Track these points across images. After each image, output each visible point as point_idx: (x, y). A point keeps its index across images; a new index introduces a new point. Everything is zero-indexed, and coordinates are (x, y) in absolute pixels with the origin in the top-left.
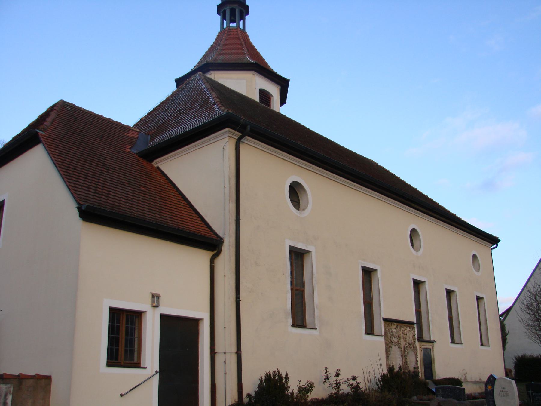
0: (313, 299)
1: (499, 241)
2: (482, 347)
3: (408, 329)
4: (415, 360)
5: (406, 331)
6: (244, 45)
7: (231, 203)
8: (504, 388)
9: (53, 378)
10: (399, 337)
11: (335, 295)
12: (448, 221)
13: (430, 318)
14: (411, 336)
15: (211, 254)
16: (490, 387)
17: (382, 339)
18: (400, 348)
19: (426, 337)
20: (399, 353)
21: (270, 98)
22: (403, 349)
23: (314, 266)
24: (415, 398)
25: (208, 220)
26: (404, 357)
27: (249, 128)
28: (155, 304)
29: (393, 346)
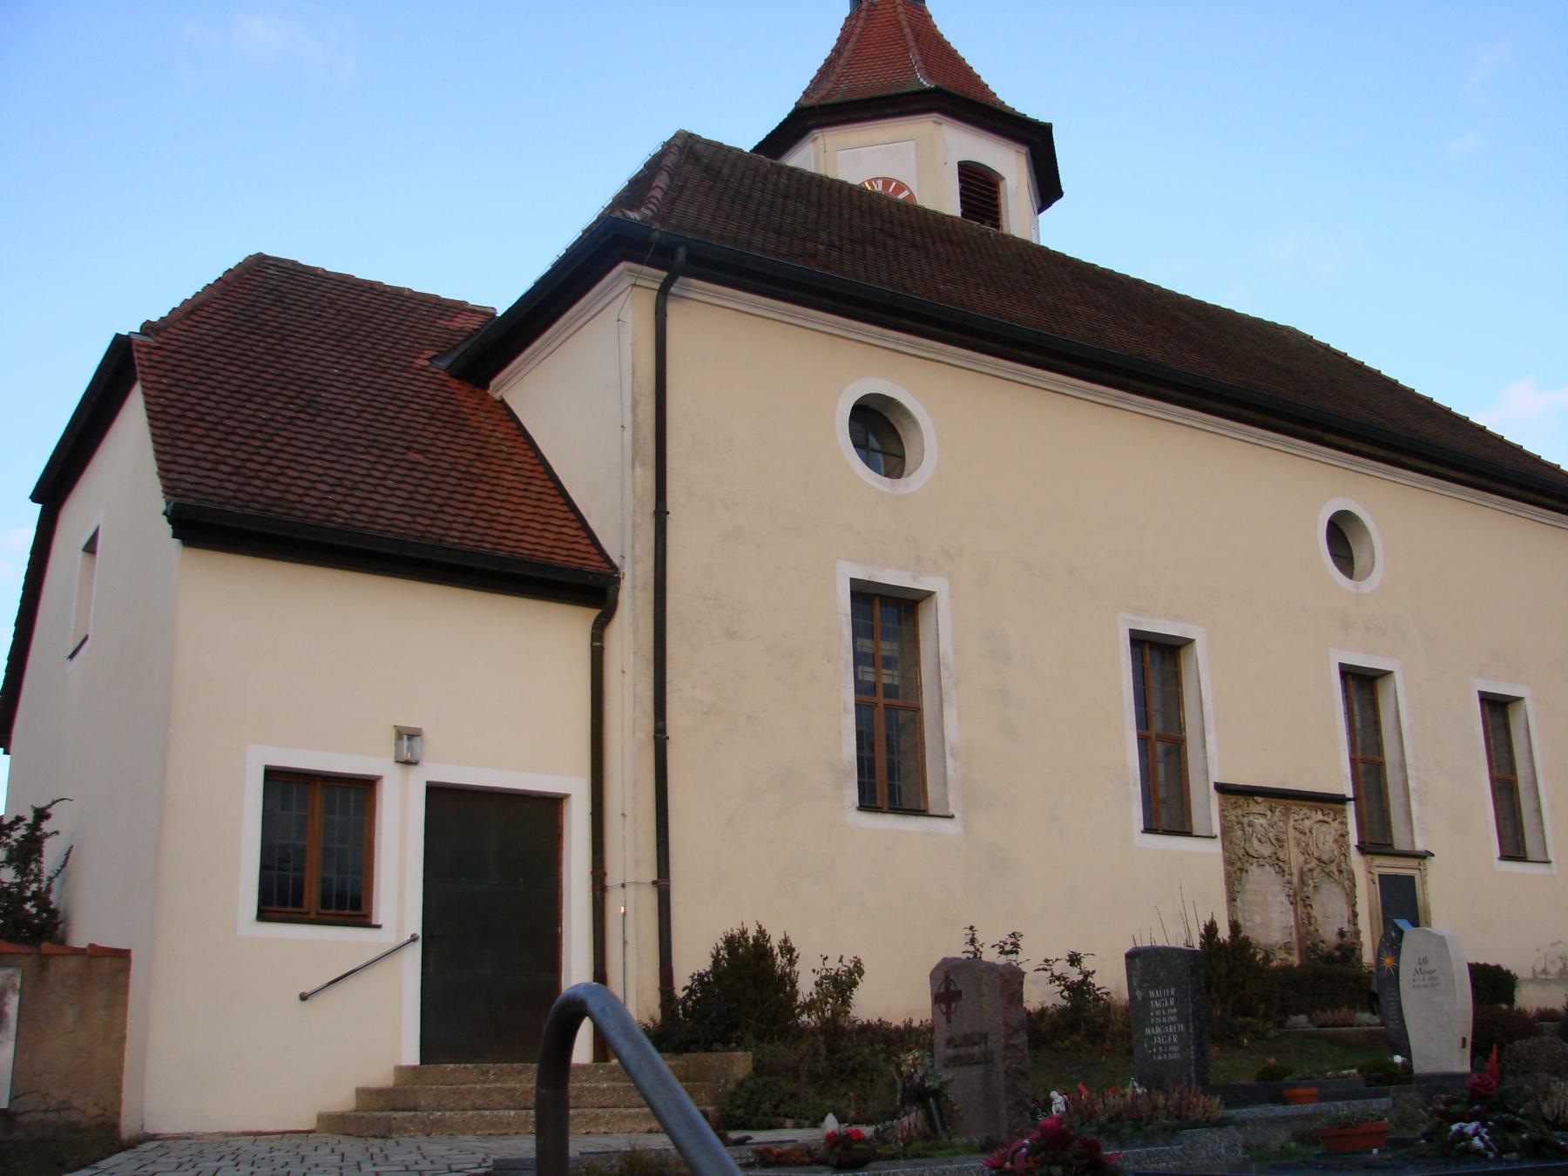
0: (942, 732)
3: (1320, 816)
4: (1345, 911)
5: (1307, 823)
6: (912, 44)
7: (639, 470)
8: (1425, 961)
9: (134, 955)
11: (1030, 720)
12: (1482, 481)
13: (1412, 784)
14: (1330, 838)
15: (591, 614)
16: (1388, 961)
17: (1216, 847)
19: (1400, 843)
22: (1295, 879)
23: (945, 635)
24: (1302, 1019)
25: (593, 523)
26: (1300, 899)
27: (681, 254)
28: (407, 756)
29: (1254, 870)
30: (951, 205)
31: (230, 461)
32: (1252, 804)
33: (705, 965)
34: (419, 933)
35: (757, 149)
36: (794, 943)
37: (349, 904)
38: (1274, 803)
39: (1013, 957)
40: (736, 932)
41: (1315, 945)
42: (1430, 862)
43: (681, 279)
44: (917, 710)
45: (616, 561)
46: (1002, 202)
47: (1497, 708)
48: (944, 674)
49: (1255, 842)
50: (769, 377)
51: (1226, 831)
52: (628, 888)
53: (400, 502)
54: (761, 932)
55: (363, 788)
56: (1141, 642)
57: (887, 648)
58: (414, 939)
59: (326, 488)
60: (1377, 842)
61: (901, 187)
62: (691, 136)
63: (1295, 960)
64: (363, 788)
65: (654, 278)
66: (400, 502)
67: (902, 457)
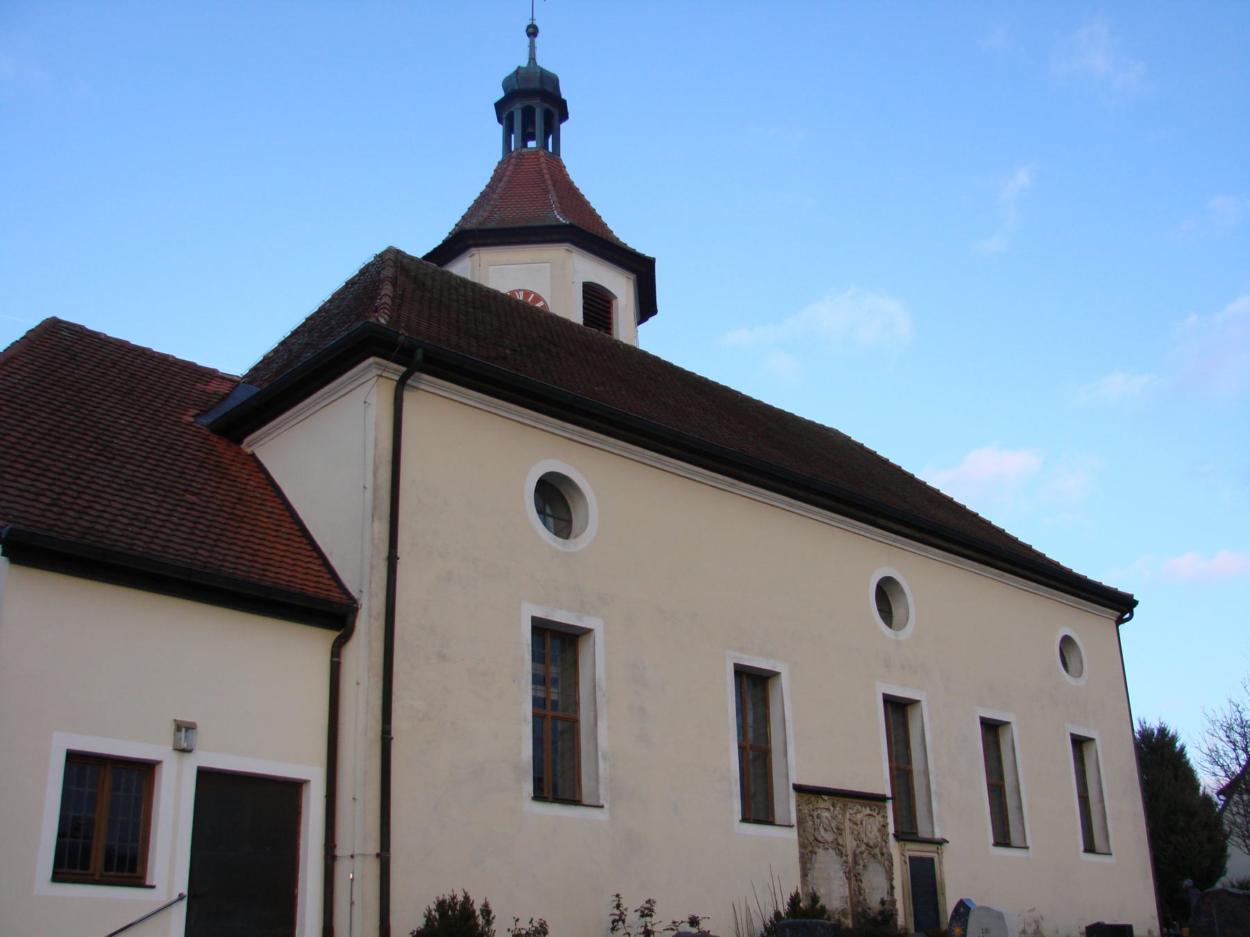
1: (1135, 603)
2: (1090, 857)
3: (868, 811)
4: (886, 885)
5: (859, 816)
6: (550, 187)
7: (377, 523)
10: (838, 829)
11: (660, 731)
12: (983, 557)
13: (933, 787)
14: (875, 828)
15: (333, 635)
17: (792, 835)
18: (841, 854)
19: (923, 832)
20: (838, 866)
21: (610, 302)
22: (850, 859)
23: (601, 665)
25: (334, 562)
26: (853, 875)
27: (419, 355)
28: (184, 745)
29: (820, 851)
30: (574, 313)
31: (48, 493)
32: (820, 801)
33: (420, 923)
34: (186, 893)
35: (425, 258)
36: (491, 907)
37: (127, 867)
38: (836, 799)
39: (648, 919)
40: (447, 898)
41: (864, 911)
42: (945, 847)
43: (417, 374)
44: (574, 722)
45: (355, 594)
46: (614, 316)
47: (992, 729)
48: (598, 694)
49: (822, 830)
50: (475, 452)
51: (801, 821)
52: (358, 860)
53: (184, 536)
54: (467, 898)
55: (146, 770)
56: (742, 673)
57: (554, 671)
58: (181, 897)
59: (126, 521)
60: (907, 833)
61: (538, 298)
62: (399, 252)
63: (849, 922)
64: (146, 770)
65: (395, 372)
66: (184, 536)
67: (570, 522)
